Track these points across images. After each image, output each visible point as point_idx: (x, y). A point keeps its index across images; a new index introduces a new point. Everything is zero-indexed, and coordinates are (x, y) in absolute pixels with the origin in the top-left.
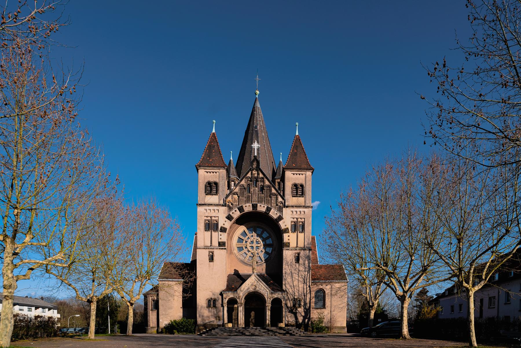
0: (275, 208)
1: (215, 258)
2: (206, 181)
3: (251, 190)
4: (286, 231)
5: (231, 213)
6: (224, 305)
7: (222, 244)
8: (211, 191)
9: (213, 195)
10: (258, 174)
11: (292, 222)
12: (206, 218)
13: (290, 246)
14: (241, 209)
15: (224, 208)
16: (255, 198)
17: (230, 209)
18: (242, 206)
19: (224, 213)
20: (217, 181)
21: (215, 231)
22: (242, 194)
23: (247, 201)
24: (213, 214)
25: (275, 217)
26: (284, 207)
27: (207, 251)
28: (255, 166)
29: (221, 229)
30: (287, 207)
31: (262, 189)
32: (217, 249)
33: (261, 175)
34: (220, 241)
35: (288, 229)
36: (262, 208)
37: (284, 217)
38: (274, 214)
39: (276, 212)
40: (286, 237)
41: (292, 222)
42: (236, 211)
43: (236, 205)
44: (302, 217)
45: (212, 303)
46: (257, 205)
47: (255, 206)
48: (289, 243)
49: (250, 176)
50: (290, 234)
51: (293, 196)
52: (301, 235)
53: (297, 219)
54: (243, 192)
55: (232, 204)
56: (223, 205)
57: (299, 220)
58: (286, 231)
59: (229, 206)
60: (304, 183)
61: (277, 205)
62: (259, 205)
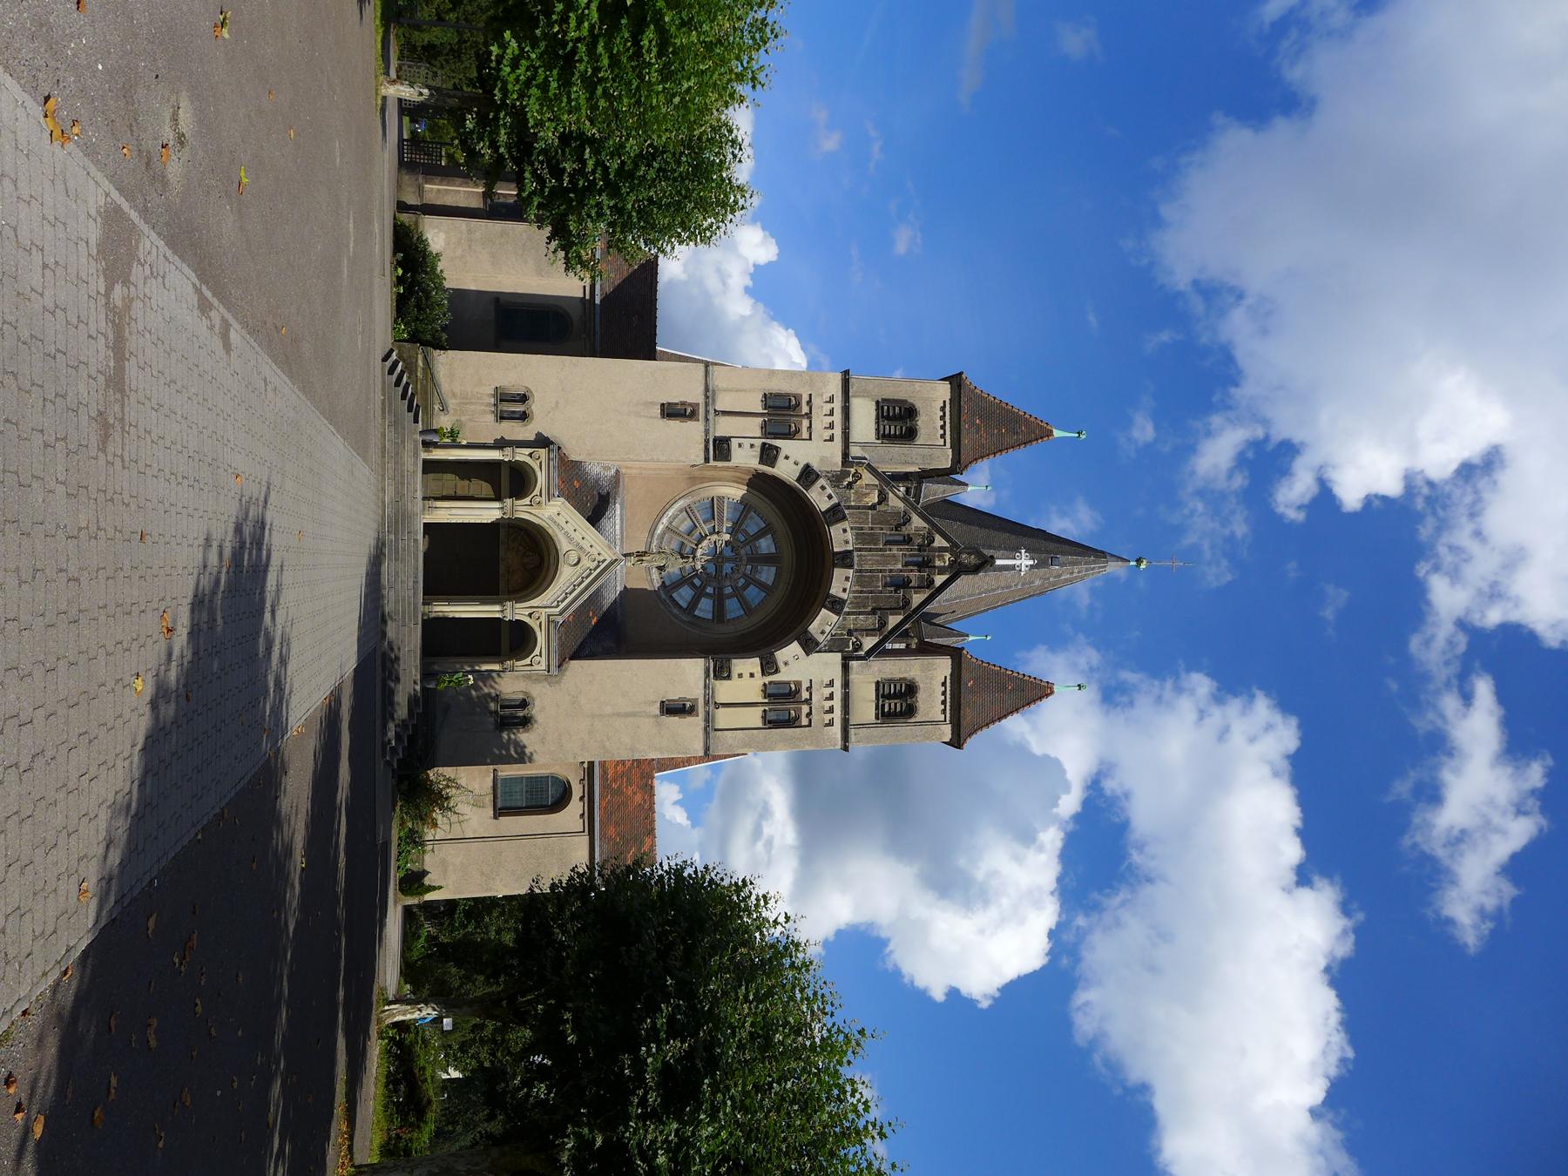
1: (675, 424)
2: (918, 405)
4: (769, 666)
5: (822, 482)
6: (508, 450)
7: (721, 448)
8: (888, 418)
9: (878, 423)
10: (942, 571)
11: (798, 684)
12: (805, 399)
13: (718, 683)
14: (836, 514)
15: (839, 459)
16: (869, 561)
17: (836, 479)
18: (844, 518)
19: (823, 460)
20: (920, 440)
21: (764, 426)
22: (881, 519)
23: (861, 536)
24: (820, 421)
25: (814, 628)
26: (844, 658)
27: (701, 400)
28: (968, 559)
30: (846, 668)
31: (902, 584)
32: (707, 432)
33: (939, 580)
34: (734, 443)
35: (777, 671)
36: (841, 583)
37: (815, 656)
38: (823, 623)
39: (828, 629)
40: (747, 666)
41: (798, 684)
42: (830, 497)
43: (848, 499)
44: (814, 717)
45: (512, 404)
46: (851, 566)
48: (729, 677)
50: (760, 680)
52: (754, 717)
53: (808, 701)
54: (887, 522)
55: (850, 485)
56: (845, 455)
57: (805, 709)
58: (769, 666)
59: (844, 474)
60: (918, 718)
61: (850, 633)
62: (850, 572)
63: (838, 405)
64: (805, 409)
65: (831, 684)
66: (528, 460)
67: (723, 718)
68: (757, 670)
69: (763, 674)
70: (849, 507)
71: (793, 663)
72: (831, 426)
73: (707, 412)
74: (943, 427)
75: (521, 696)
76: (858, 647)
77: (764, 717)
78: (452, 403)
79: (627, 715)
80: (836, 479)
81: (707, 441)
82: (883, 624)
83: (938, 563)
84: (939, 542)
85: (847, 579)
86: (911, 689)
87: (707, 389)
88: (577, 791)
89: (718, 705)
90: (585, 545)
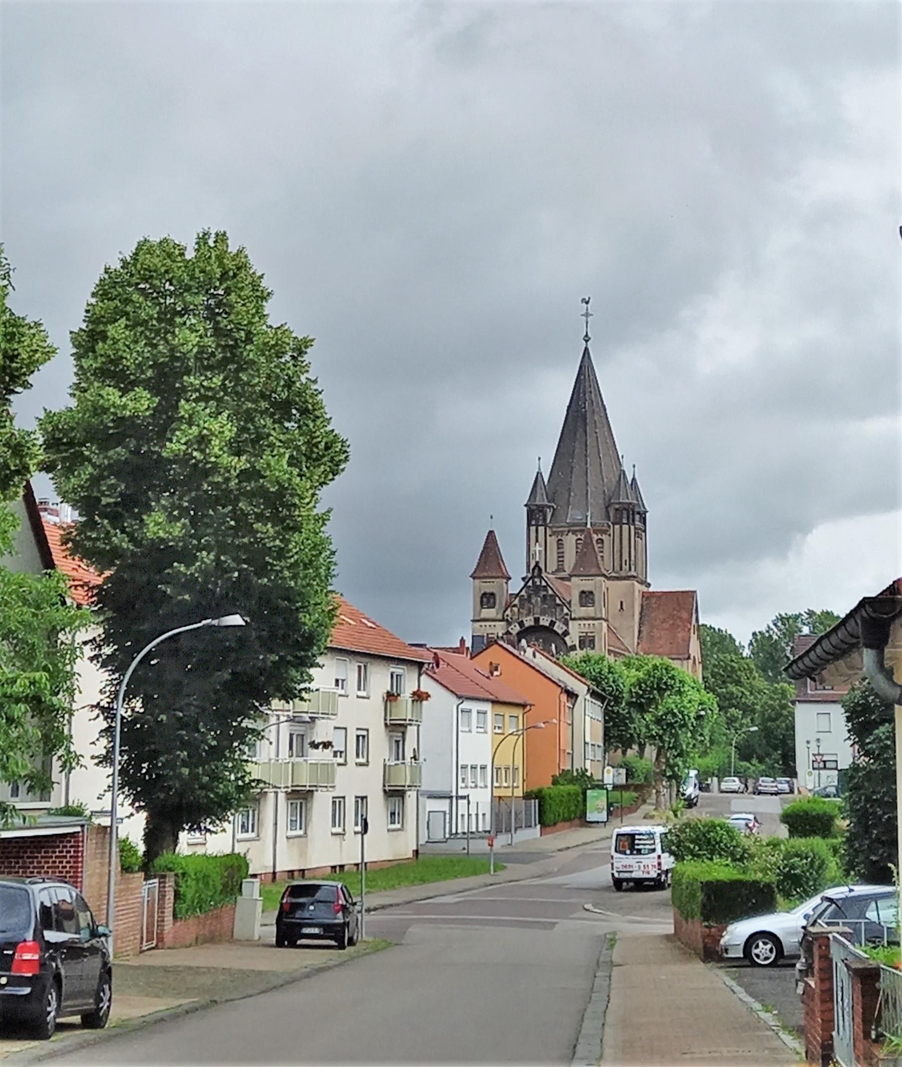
0: (560, 621)
14: (521, 624)
17: (509, 624)
18: (522, 621)
20: (494, 591)
22: (522, 606)
23: (528, 615)
30: (575, 619)
36: (545, 621)
37: (570, 631)
47: (537, 620)
56: (500, 621)
59: (507, 620)
62: (541, 618)
63: (483, 624)
76: (567, 614)
80: (509, 624)
82: (559, 605)
84: (530, 583)
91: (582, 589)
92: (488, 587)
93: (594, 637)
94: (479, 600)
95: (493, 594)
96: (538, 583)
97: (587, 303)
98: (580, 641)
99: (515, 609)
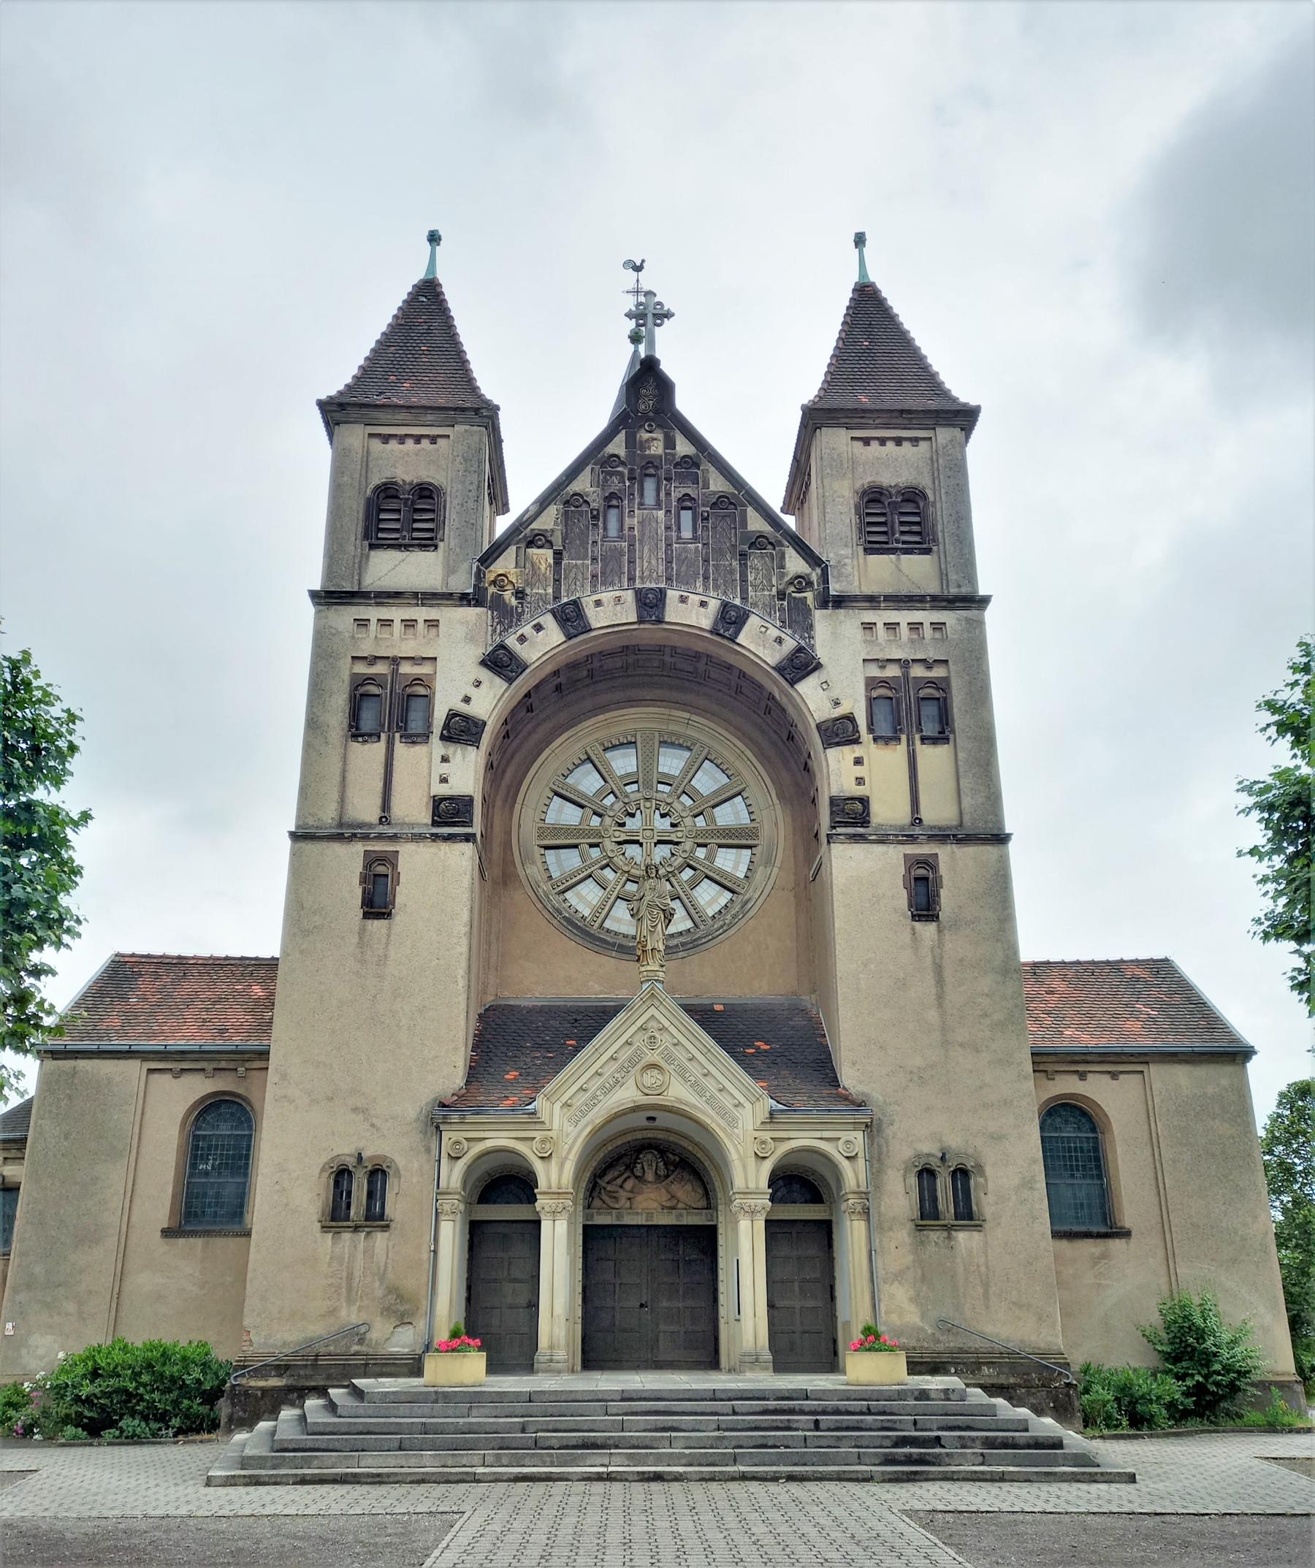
0: (769, 610)
1: (404, 895)
3: (627, 521)
5: (511, 642)
10: (670, 443)
11: (871, 683)
14: (571, 618)
15: (472, 613)
17: (506, 616)
18: (576, 604)
19: (471, 639)
21: (411, 739)
27: (359, 848)
29: (446, 726)
30: (840, 602)
32: (417, 838)
35: (850, 718)
36: (691, 612)
37: (821, 652)
38: (762, 642)
39: (774, 632)
40: (839, 771)
42: (538, 628)
43: (543, 598)
44: (932, 655)
46: (662, 593)
47: (651, 604)
48: (864, 801)
49: (622, 452)
50: (867, 748)
51: (867, 551)
52: (934, 759)
53: (905, 664)
54: (583, 536)
56: (465, 600)
57: (918, 671)
58: (840, 732)
59: (497, 605)
62: (672, 595)
63: (374, 613)
64: (381, 668)
65: (869, 627)
66: (460, 1166)
67: (937, 811)
68: (848, 753)
69: (856, 741)
70: (557, 598)
71: (835, 689)
72: (409, 624)
73: (380, 837)
74: (418, 439)
75: (913, 1181)
76: (801, 582)
77: (934, 741)
78: (350, 1315)
79: (940, 981)
80: (506, 616)
81: (435, 837)
82: (758, 542)
83: (657, 449)
85: (683, 600)
86: (873, 497)
87: (339, 837)
88: (1067, 1085)
89: (917, 821)
90: (625, 1055)
91: (866, 479)
92: (405, 462)
93: (942, 685)
94: (356, 509)
95: (426, 492)
96: (657, 449)
97: (638, 269)
98: (871, 702)
99: (543, 556)
